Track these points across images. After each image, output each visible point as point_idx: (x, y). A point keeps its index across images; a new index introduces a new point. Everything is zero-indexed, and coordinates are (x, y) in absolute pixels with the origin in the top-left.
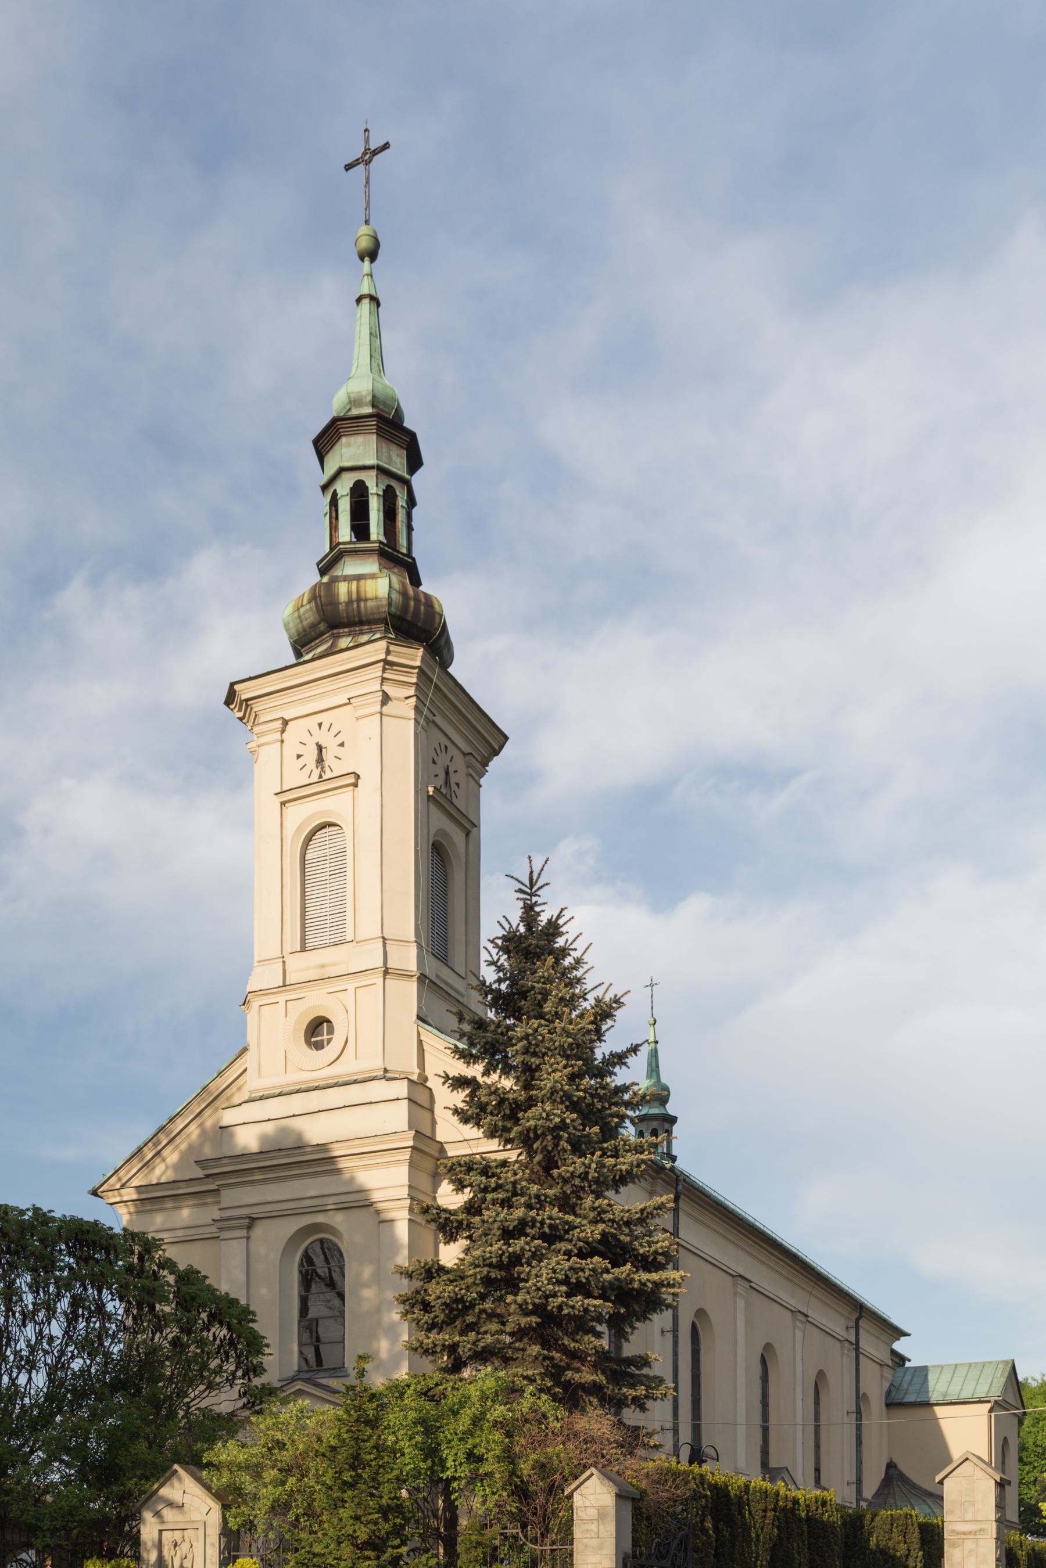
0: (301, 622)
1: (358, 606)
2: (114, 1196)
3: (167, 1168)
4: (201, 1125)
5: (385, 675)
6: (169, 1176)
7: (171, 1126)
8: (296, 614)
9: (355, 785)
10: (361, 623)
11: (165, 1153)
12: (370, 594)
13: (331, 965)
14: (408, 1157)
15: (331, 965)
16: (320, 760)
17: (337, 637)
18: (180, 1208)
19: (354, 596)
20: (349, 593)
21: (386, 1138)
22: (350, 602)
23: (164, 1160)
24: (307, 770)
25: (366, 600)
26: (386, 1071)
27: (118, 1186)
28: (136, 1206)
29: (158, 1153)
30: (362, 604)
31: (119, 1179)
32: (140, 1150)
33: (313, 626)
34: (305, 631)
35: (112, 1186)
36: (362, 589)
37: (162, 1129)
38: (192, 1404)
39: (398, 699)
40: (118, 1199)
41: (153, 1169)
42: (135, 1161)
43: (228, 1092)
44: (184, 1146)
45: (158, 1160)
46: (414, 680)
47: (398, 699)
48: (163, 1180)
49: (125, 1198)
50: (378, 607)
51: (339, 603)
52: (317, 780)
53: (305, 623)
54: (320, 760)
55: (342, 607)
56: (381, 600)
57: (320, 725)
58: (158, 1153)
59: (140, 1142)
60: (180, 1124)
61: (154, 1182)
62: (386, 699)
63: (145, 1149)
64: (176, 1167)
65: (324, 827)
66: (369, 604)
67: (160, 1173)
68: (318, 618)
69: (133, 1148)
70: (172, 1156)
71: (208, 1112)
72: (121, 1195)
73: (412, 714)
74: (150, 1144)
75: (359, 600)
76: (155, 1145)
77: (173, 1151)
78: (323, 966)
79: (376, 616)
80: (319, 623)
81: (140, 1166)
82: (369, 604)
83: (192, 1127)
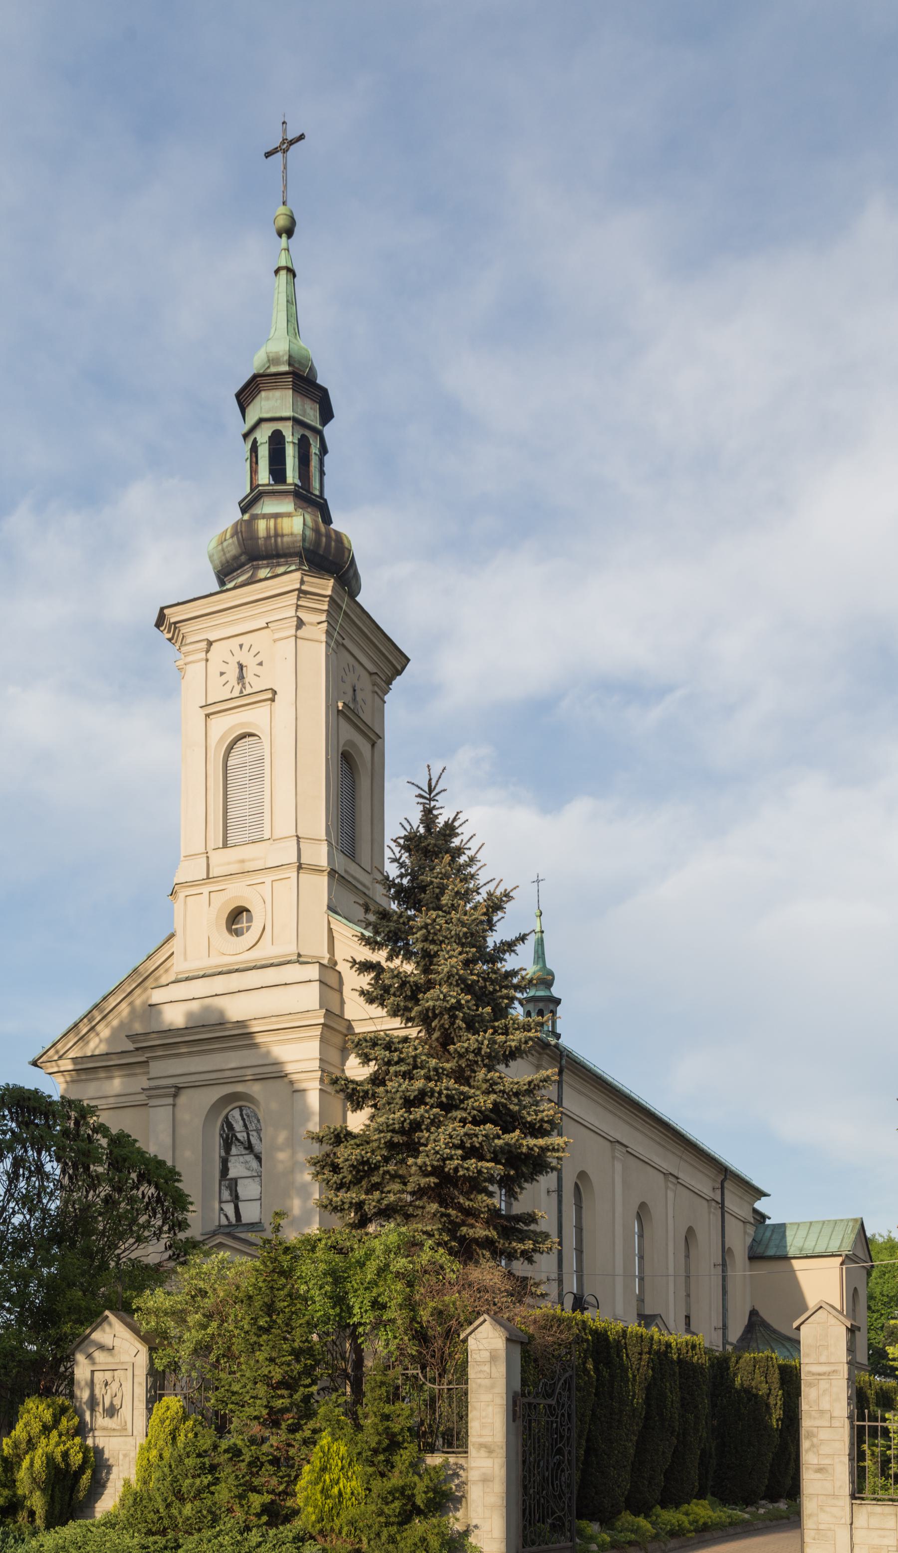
0: (224, 554)
1: (276, 541)
2: (52, 1067)
3: (101, 1041)
4: (131, 1004)
5: (300, 603)
6: (103, 1049)
7: (105, 1004)
8: (220, 548)
9: (273, 700)
10: (278, 556)
11: (99, 1028)
12: (286, 531)
13: (250, 860)
14: (319, 1033)
15: (250, 860)
16: (241, 678)
17: (257, 568)
18: (111, 1078)
19: (272, 532)
20: (268, 529)
21: (299, 1016)
22: (268, 537)
23: (98, 1034)
24: (229, 687)
25: (282, 536)
26: (299, 955)
27: (56, 1058)
28: (71, 1076)
29: (92, 1029)
30: (279, 540)
31: (57, 1052)
32: (76, 1025)
33: (235, 558)
34: (228, 562)
35: (51, 1057)
36: (279, 526)
37: (96, 1006)
38: (122, 1256)
39: (311, 624)
40: (55, 1070)
41: (88, 1042)
42: (71, 1035)
43: (157, 974)
44: (115, 1023)
45: (92, 1035)
46: (326, 607)
47: (311, 624)
48: (97, 1053)
49: (62, 1069)
50: (294, 542)
51: (258, 538)
52: (238, 695)
53: (228, 555)
54: (241, 678)
55: (261, 542)
56: (296, 536)
57: (241, 646)
58: (92, 1029)
59: (76, 1019)
60: (112, 1002)
61: (89, 1054)
62: (300, 624)
63: (81, 1025)
64: (110, 1040)
65: (245, 737)
66: (286, 539)
67: (95, 1045)
68: (239, 551)
69: (70, 1023)
70: (104, 1031)
71: (138, 991)
72: (58, 1066)
73: (323, 637)
74: (85, 1020)
75: (276, 535)
76: (90, 1021)
77: (107, 1026)
78: (243, 861)
79: (292, 550)
80: (241, 555)
81: (76, 1039)
82: (286, 539)
83: (124, 1005)
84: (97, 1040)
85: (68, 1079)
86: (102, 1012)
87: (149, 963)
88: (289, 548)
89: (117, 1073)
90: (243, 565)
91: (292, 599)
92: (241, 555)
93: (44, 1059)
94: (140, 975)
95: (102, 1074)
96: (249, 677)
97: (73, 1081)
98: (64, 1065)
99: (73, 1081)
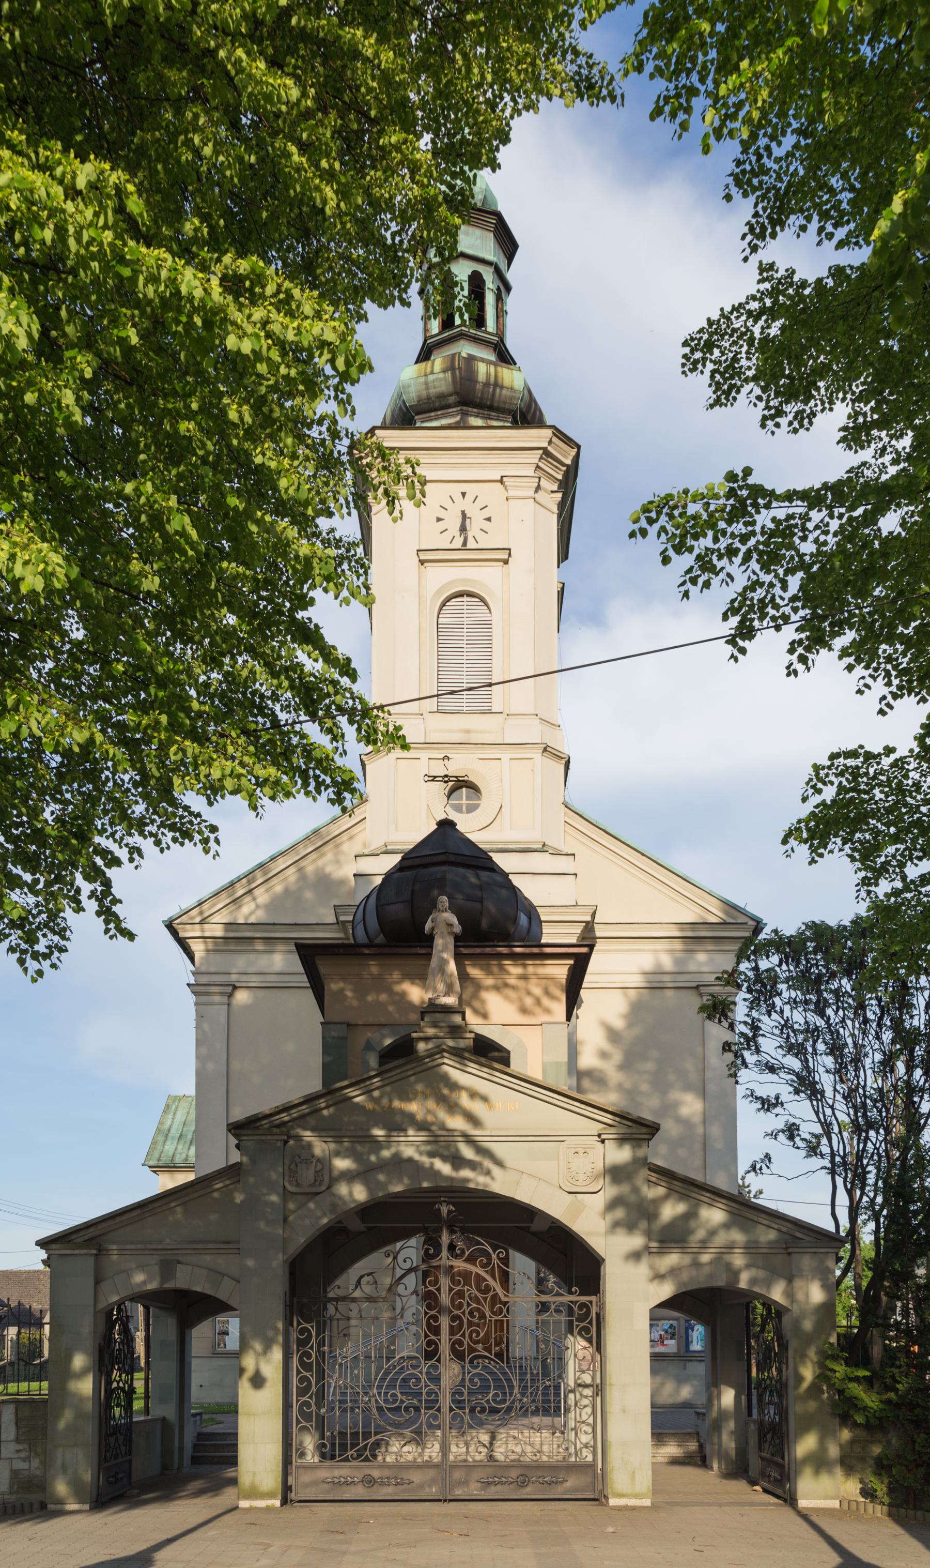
0: (427, 388)
1: (494, 391)
2: (193, 930)
3: (258, 907)
4: (300, 870)
5: (540, 464)
6: (259, 916)
7: (272, 865)
8: (422, 380)
9: (506, 562)
10: (491, 408)
11: (257, 892)
12: (507, 383)
13: (477, 732)
14: (579, 931)
15: (477, 732)
16: (463, 529)
17: (465, 414)
18: (272, 952)
19: (492, 380)
20: (488, 375)
21: (564, 910)
22: (487, 384)
23: (254, 899)
24: (448, 536)
25: (502, 387)
26: (544, 845)
27: (198, 920)
28: (216, 944)
29: (250, 891)
30: (498, 390)
31: (201, 913)
32: (232, 884)
33: (442, 396)
34: (429, 398)
35: (192, 918)
36: (500, 375)
37: (261, 866)
38: (835, 1149)
39: (546, 491)
40: (198, 934)
41: (240, 907)
42: (224, 895)
43: (338, 840)
44: (279, 888)
45: (248, 899)
46: (560, 477)
47: (546, 491)
48: (252, 920)
49: (207, 934)
50: (511, 398)
51: (477, 382)
52: (459, 547)
53: (432, 391)
54: (463, 529)
55: (479, 387)
56: (515, 391)
57: (464, 494)
58: (250, 891)
59: (232, 876)
60: (281, 864)
61: (241, 921)
62: (538, 488)
63: (238, 885)
64: (270, 907)
65: (462, 596)
66: (504, 392)
67: (249, 912)
68: (451, 389)
69: (225, 881)
70: (262, 896)
71: (313, 856)
72: (203, 931)
73: (555, 509)
74: (244, 881)
75: (496, 384)
76: (249, 882)
77: (267, 891)
78: (468, 731)
79: (507, 406)
80: (451, 395)
81: (228, 901)
82: (504, 392)
83: (292, 870)
84: (252, 906)
85: (211, 947)
86: (265, 874)
87: (332, 827)
88: (505, 403)
89: (281, 947)
90: (448, 406)
91: (534, 457)
92: (451, 395)
93: (184, 919)
94: (322, 837)
95: (259, 946)
96: (474, 530)
97: (214, 951)
98: (212, 930)
99: (214, 951)
